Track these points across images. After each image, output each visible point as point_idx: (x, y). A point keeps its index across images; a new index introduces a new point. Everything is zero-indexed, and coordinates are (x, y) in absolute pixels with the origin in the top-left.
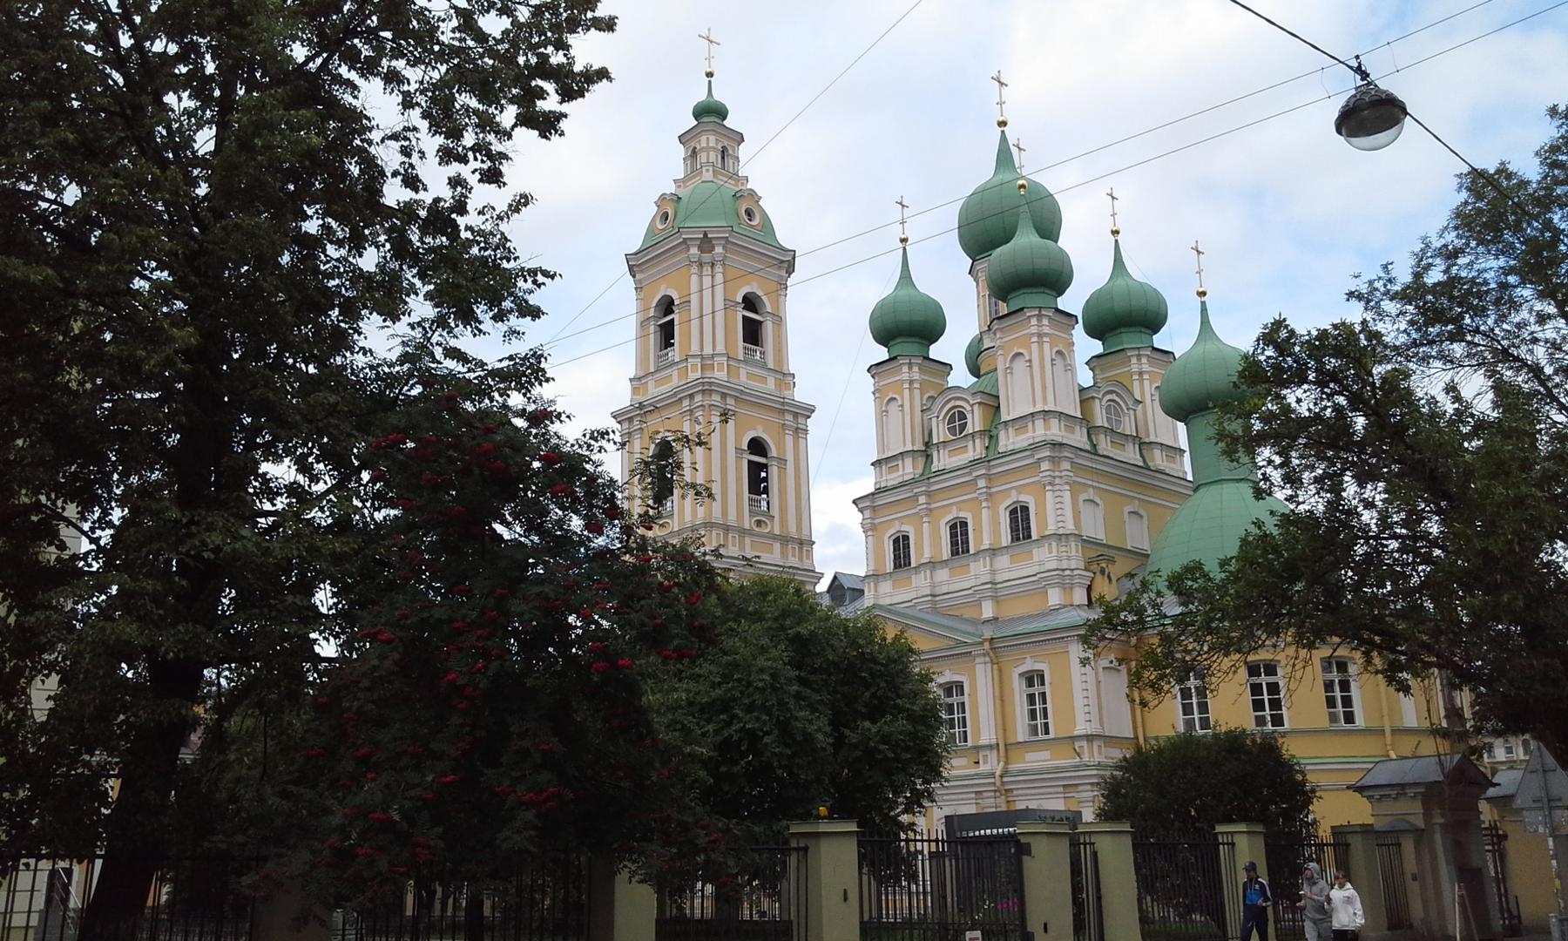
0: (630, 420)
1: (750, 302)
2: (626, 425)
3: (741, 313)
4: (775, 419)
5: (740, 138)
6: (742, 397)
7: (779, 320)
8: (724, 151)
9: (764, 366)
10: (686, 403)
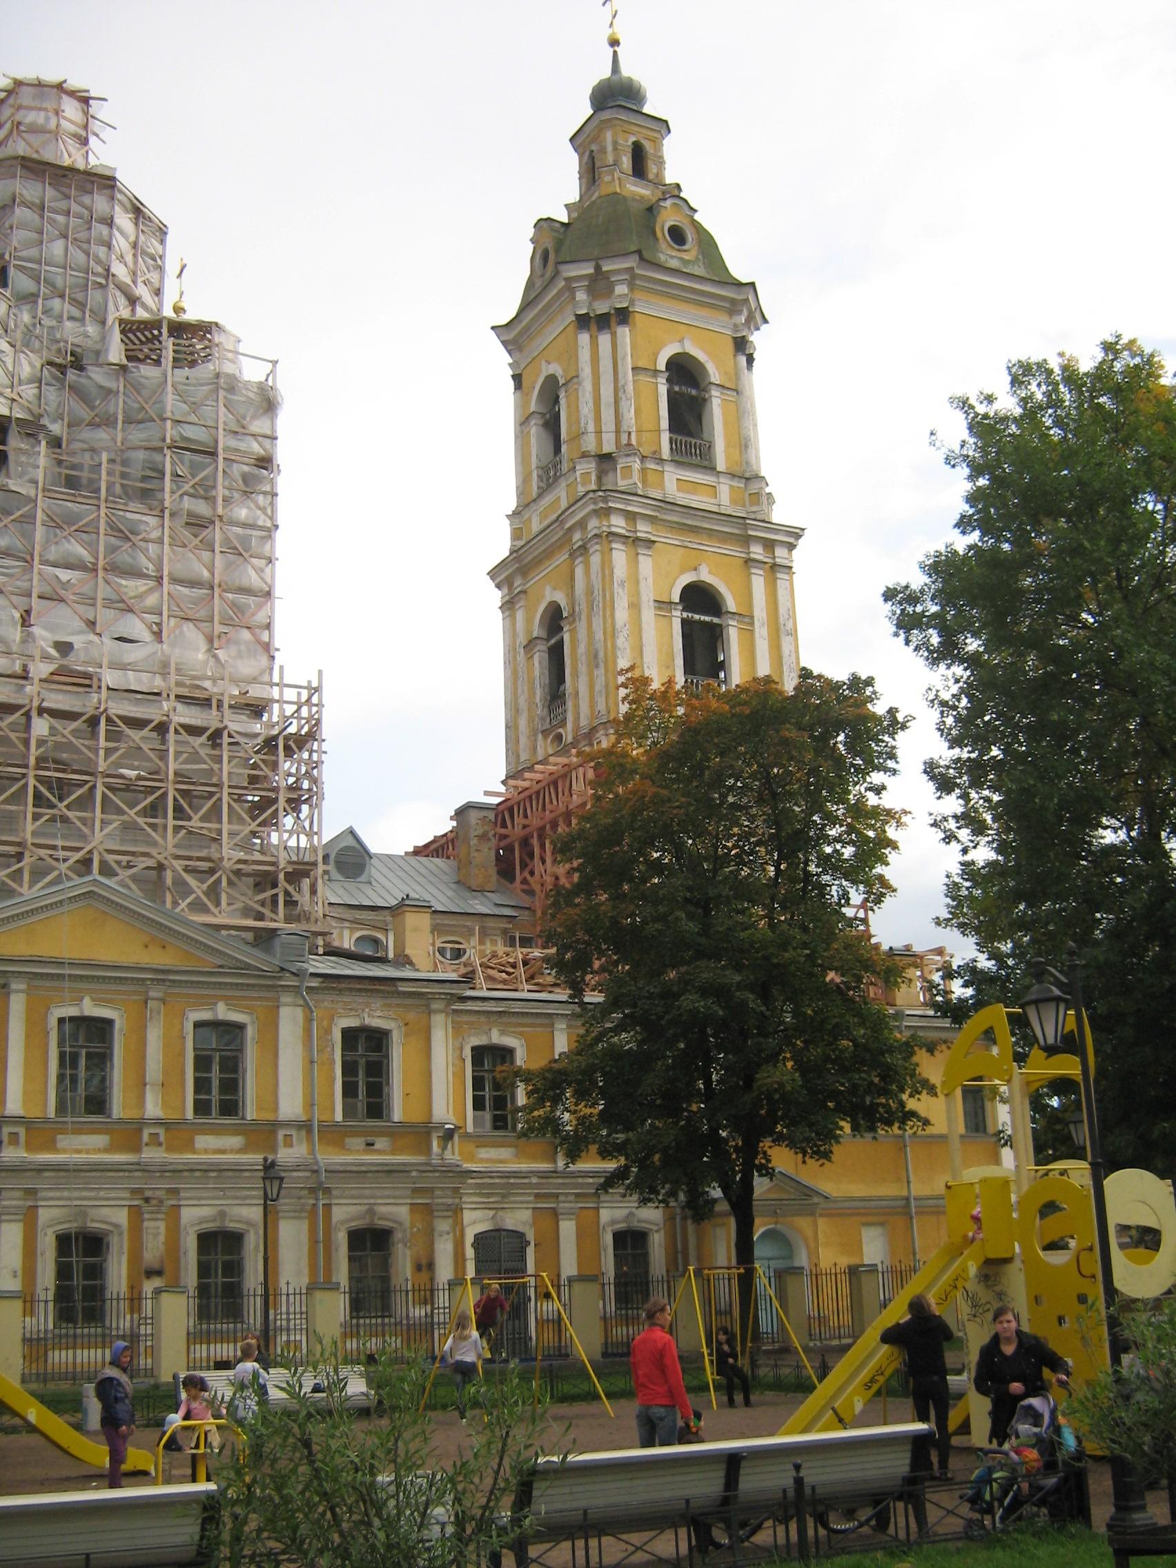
10: (577, 536)
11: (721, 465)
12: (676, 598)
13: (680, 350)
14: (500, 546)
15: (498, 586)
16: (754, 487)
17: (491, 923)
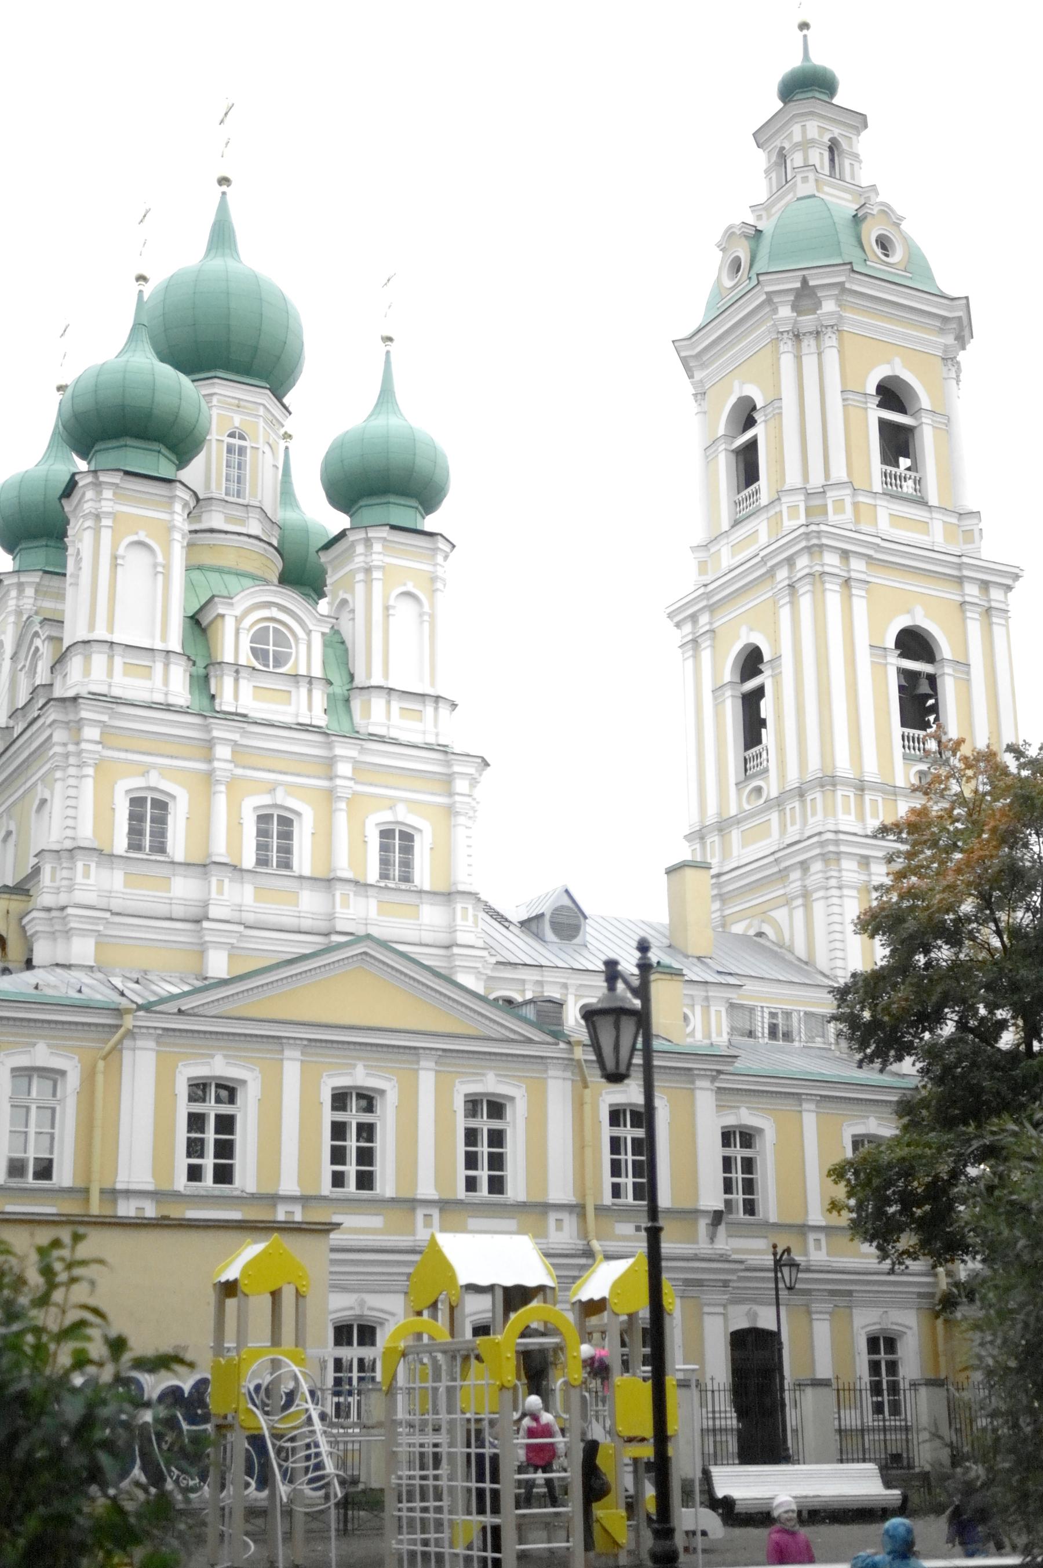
0: (694, 618)
1: (891, 395)
2: (688, 628)
3: (876, 414)
5: (859, 121)
6: (883, 558)
7: (945, 421)
8: (833, 148)
9: (921, 501)
10: (782, 574)
12: (890, 642)
13: (890, 373)
14: (684, 581)
15: (678, 625)
16: (968, 523)
17: (713, 992)
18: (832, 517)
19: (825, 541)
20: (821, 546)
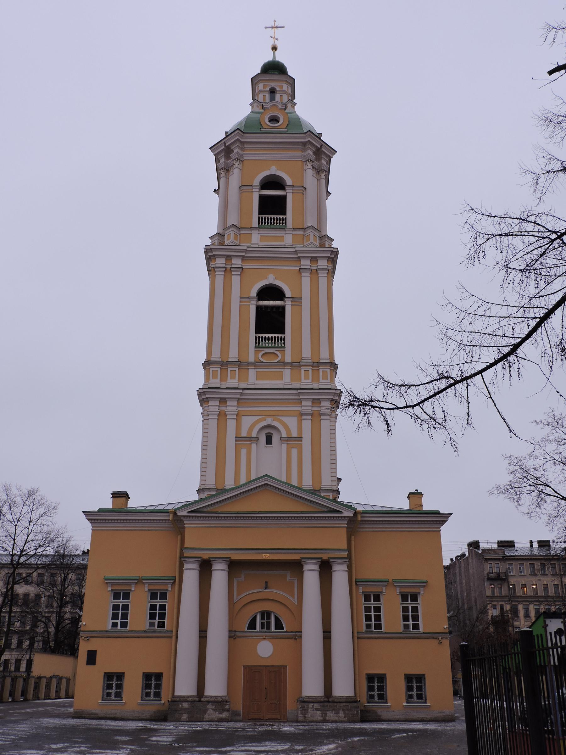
4: (293, 267)
11: (289, 224)
12: (254, 293)
18: (226, 243)
19: (214, 253)
20: (214, 256)
